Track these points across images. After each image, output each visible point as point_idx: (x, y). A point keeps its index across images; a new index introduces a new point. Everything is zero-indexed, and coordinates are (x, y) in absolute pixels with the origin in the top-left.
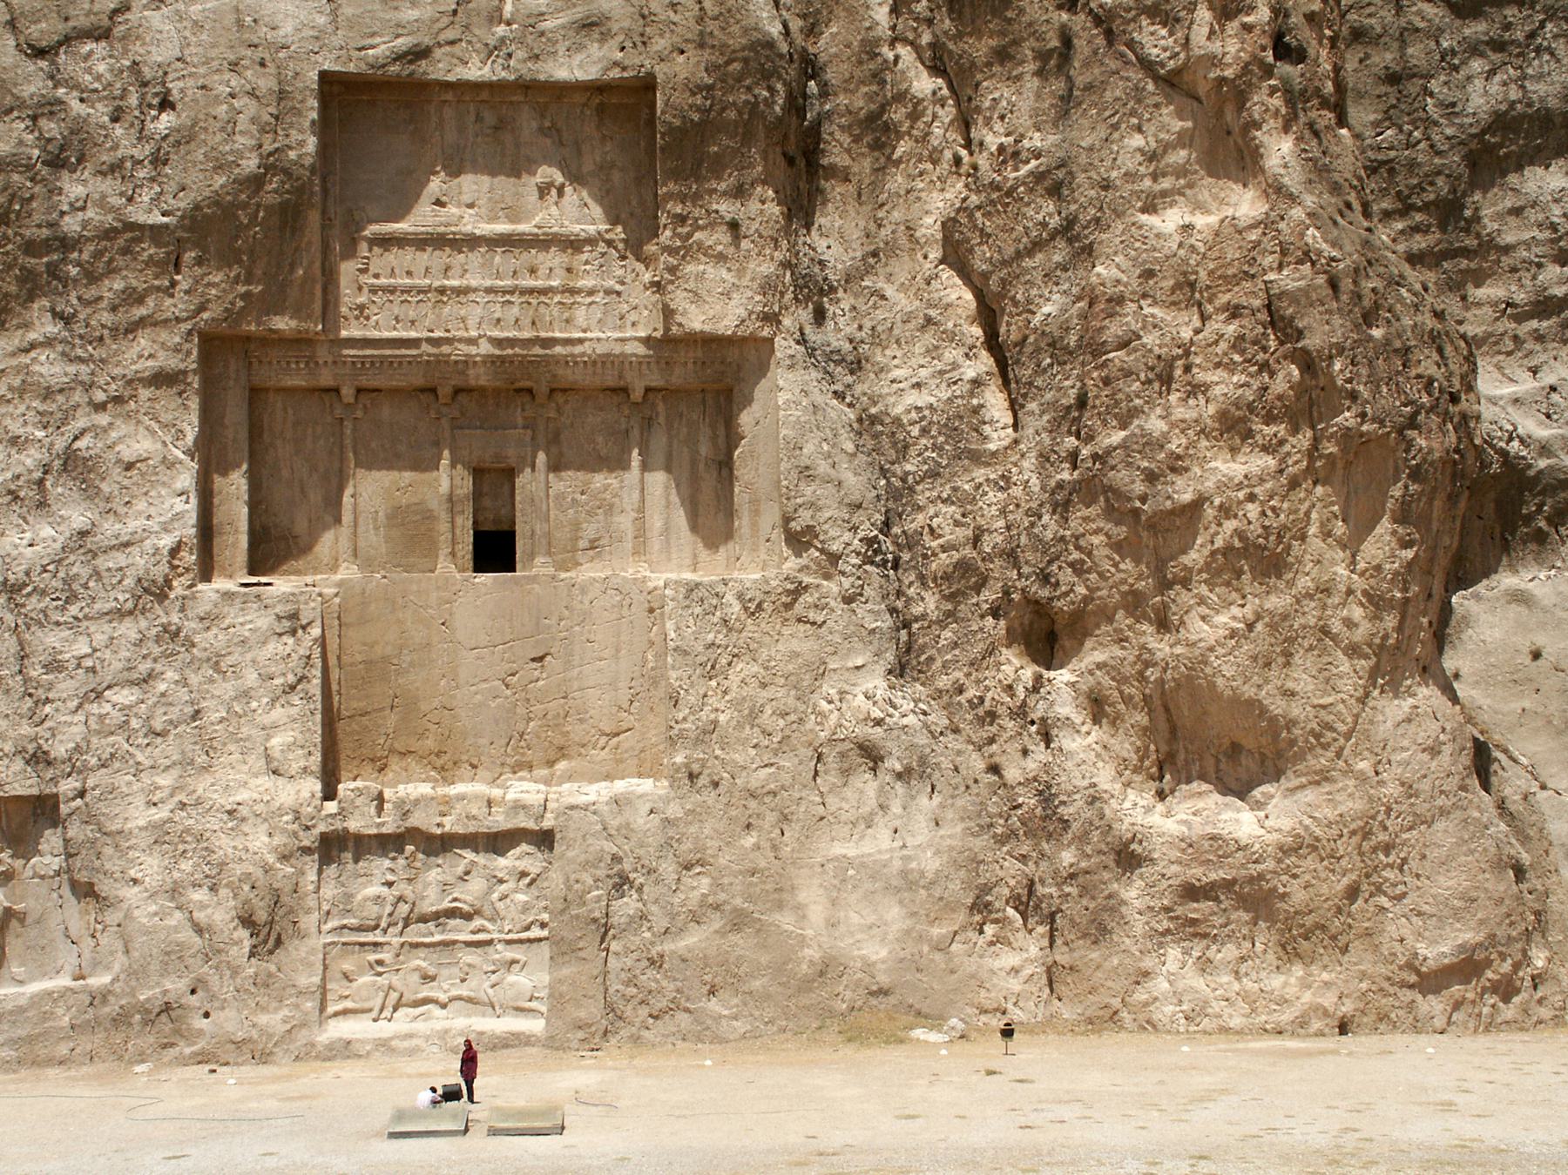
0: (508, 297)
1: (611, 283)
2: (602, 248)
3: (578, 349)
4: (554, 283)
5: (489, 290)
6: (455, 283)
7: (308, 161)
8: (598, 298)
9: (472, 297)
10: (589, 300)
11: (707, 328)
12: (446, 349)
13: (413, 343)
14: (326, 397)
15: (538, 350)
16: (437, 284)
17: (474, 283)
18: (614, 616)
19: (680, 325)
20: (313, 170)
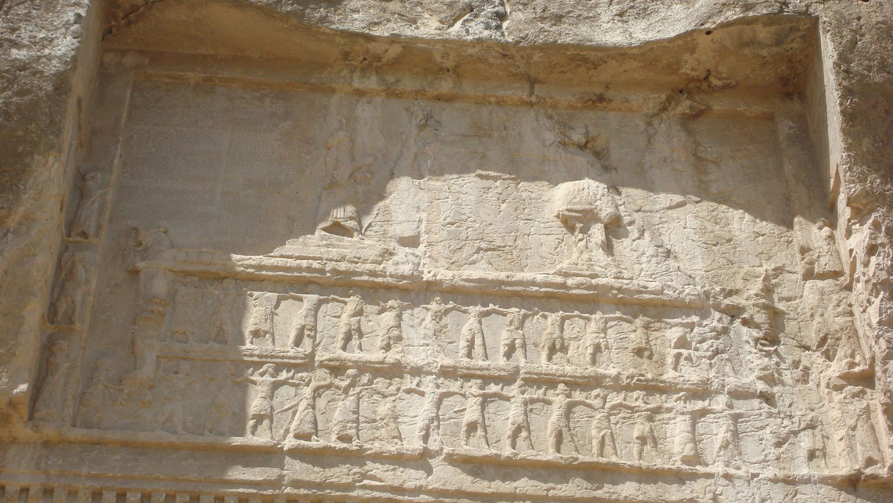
1: (750, 379)
2: (715, 320)
5: (447, 373)
6: (375, 355)
7: (55, 66)
8: (720, 402)
9: (409, 382)
10: (699, 405)
12: (340, 474)
16: (321, 356)
17: (416, 357)
20: (62, 83)
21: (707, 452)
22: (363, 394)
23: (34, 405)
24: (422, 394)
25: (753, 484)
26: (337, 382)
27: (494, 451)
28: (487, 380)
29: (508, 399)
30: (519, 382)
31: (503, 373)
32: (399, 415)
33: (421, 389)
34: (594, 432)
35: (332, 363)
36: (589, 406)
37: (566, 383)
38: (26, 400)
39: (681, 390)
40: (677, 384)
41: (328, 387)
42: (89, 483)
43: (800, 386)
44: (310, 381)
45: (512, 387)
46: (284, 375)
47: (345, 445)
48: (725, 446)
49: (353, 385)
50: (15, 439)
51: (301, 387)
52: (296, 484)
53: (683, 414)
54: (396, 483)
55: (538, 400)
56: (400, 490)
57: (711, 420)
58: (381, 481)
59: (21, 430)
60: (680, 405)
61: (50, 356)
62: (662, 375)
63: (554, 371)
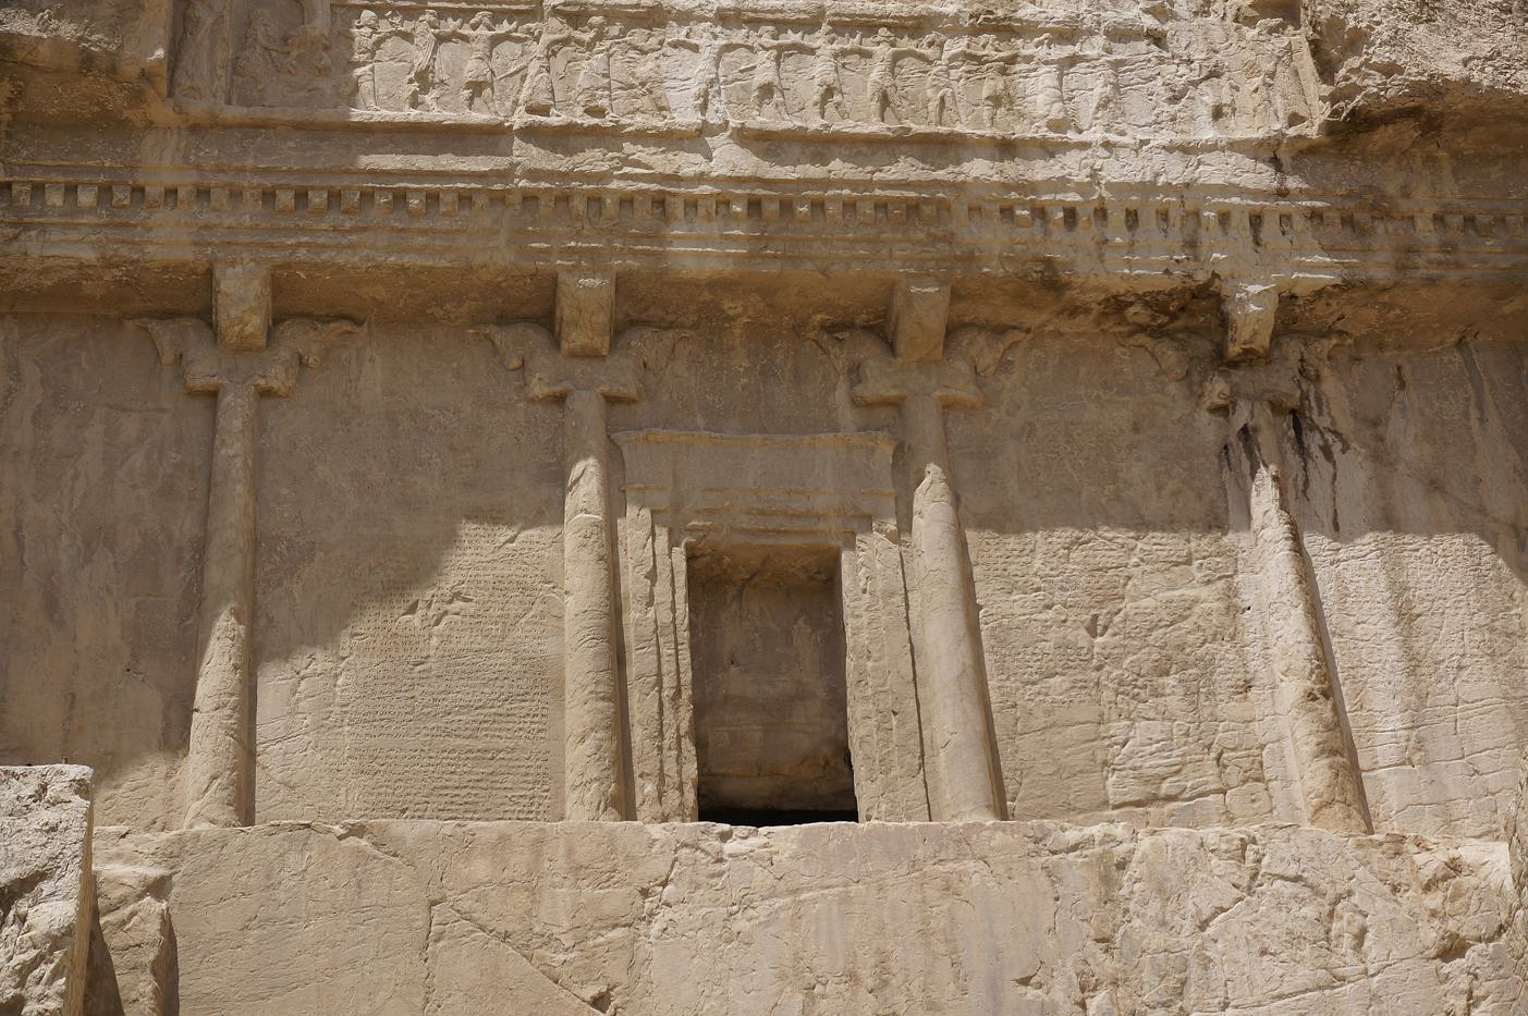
0: (792, 37)
3: (1040, 171)
4: (951, 9)
8: (1094, 47)
9: (678, 33)
10: (1067, 50)
11: (1484, 77)
12: (593, 160)
13: (490, 137)
14: (164, 334)
15: (905, 169)
18: (1303, 975)
19: (1389, 70)
21: (1081, 114)
22: (614, 49)
23: (172, 76)
24: (695, 48)
25: (1142, 154)
26: (577, 34)
27: (799, 124)
28: (781, 25)
29: (812, 51)
30: (825, 27)
31: (803, 16)
32: (666, 78)
33: (693, 41)
34: (929, 93)
35: (568, 8)
36: (921, 57)
37: (889, 27)
38: (164, 71)
39: (1045, 31)
40: (1038, 23)
41: (565, 42)
42: (256, 180)
43: (1199, 20)
44: (540, 33)
45: (817, 34)
46: (504, 27)
47: (596, 121)
48: (1103, 105)
49: (600, 37)
50: (152, 123)
51: (529, 43)
52: (534, 175)
53: (1047, 63)
54: (669, 170)
55: (852, 52)
56: (675, 178)
57: (1083, 71)
58: (647, 167)
59: (161, 111)
60: (1042, 52)
61: (186, 9)
62: (1016, 11)
63: (872, 11)
